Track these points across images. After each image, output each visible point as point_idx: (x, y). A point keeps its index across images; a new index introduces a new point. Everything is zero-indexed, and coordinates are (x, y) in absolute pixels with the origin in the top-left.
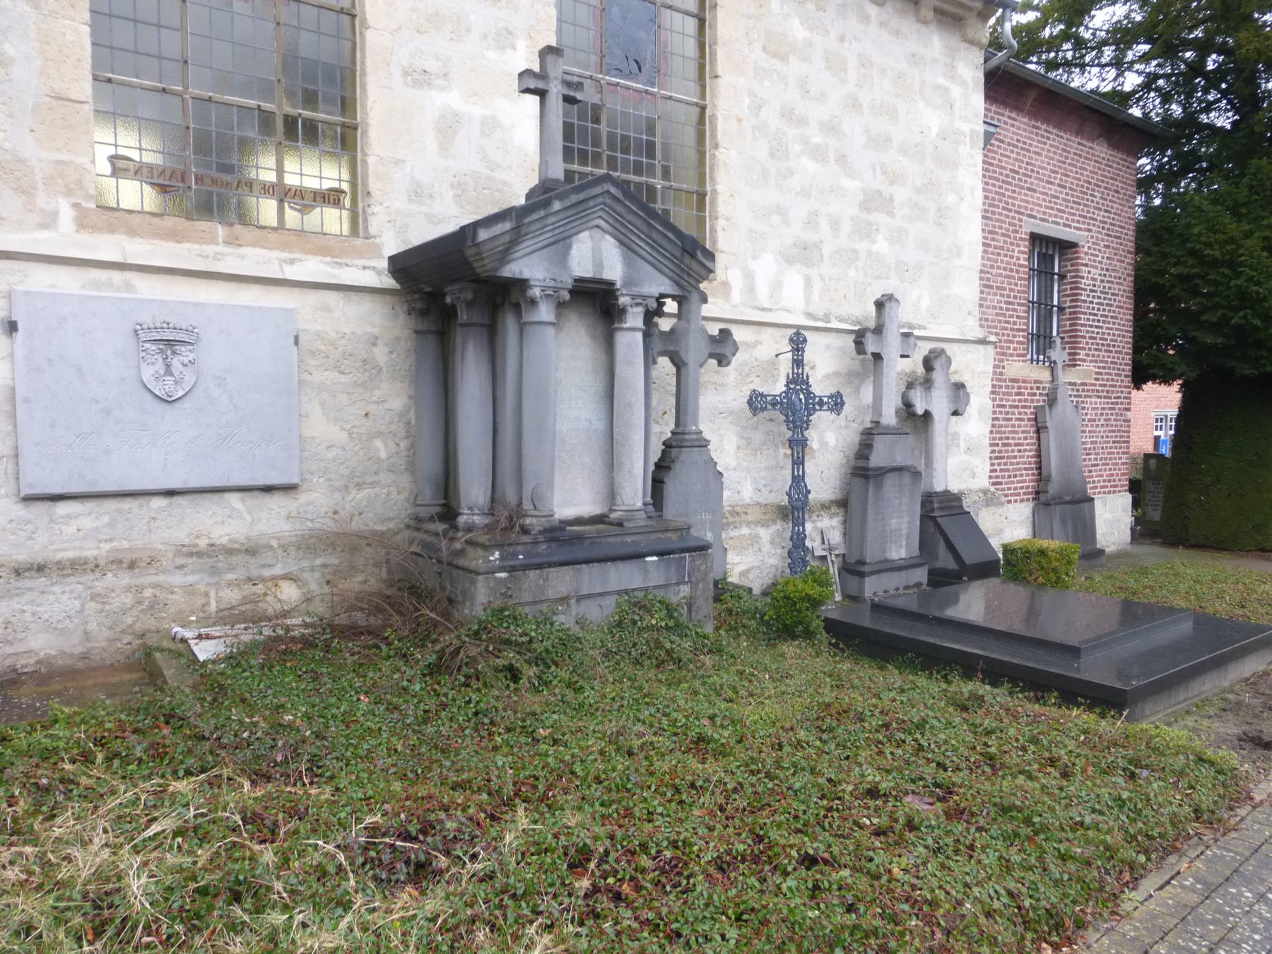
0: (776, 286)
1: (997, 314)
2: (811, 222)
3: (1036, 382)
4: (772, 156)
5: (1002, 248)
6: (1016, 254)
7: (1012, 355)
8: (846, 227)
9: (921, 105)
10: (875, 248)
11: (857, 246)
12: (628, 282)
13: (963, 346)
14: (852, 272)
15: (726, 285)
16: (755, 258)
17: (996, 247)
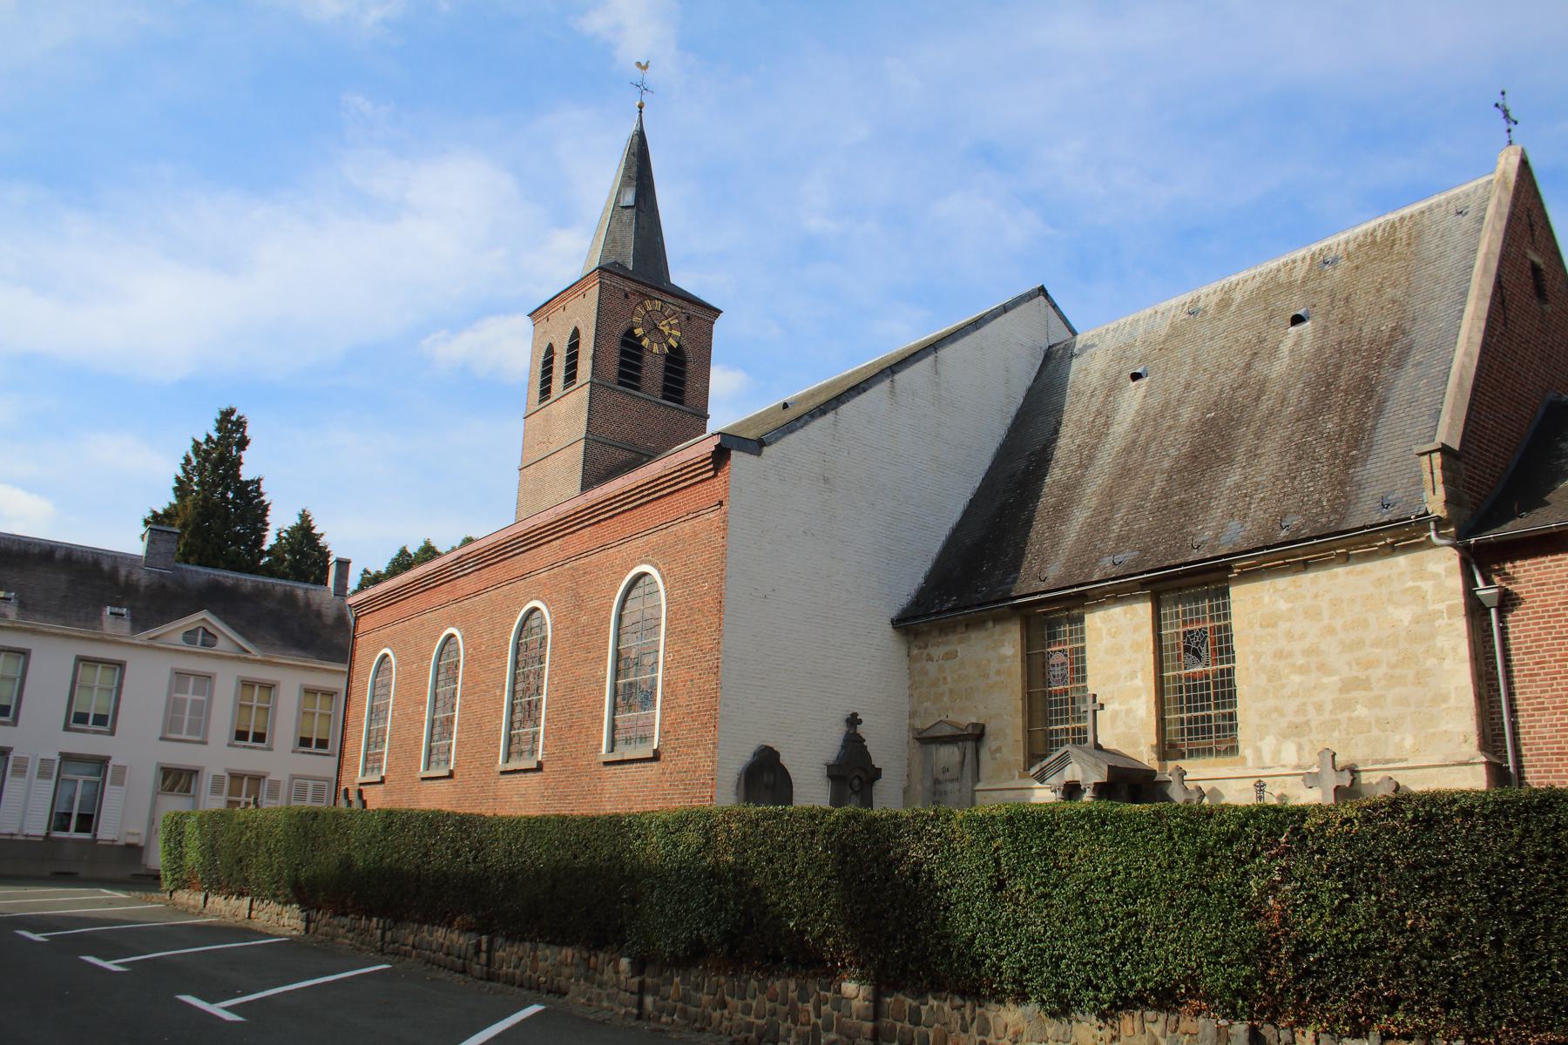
1: (1557, 731)
2: (1301, 710)
4: (1269, 680)
8: (1329, 707)
9: (1391, 609)
10: (1355, 714)
11: (1339, 717)
12: (1083, 780)
13: (1446, 770)
14: (1336, 734)
15: (1244, 758)
16: (1262, 739)
17: (1546, 674)
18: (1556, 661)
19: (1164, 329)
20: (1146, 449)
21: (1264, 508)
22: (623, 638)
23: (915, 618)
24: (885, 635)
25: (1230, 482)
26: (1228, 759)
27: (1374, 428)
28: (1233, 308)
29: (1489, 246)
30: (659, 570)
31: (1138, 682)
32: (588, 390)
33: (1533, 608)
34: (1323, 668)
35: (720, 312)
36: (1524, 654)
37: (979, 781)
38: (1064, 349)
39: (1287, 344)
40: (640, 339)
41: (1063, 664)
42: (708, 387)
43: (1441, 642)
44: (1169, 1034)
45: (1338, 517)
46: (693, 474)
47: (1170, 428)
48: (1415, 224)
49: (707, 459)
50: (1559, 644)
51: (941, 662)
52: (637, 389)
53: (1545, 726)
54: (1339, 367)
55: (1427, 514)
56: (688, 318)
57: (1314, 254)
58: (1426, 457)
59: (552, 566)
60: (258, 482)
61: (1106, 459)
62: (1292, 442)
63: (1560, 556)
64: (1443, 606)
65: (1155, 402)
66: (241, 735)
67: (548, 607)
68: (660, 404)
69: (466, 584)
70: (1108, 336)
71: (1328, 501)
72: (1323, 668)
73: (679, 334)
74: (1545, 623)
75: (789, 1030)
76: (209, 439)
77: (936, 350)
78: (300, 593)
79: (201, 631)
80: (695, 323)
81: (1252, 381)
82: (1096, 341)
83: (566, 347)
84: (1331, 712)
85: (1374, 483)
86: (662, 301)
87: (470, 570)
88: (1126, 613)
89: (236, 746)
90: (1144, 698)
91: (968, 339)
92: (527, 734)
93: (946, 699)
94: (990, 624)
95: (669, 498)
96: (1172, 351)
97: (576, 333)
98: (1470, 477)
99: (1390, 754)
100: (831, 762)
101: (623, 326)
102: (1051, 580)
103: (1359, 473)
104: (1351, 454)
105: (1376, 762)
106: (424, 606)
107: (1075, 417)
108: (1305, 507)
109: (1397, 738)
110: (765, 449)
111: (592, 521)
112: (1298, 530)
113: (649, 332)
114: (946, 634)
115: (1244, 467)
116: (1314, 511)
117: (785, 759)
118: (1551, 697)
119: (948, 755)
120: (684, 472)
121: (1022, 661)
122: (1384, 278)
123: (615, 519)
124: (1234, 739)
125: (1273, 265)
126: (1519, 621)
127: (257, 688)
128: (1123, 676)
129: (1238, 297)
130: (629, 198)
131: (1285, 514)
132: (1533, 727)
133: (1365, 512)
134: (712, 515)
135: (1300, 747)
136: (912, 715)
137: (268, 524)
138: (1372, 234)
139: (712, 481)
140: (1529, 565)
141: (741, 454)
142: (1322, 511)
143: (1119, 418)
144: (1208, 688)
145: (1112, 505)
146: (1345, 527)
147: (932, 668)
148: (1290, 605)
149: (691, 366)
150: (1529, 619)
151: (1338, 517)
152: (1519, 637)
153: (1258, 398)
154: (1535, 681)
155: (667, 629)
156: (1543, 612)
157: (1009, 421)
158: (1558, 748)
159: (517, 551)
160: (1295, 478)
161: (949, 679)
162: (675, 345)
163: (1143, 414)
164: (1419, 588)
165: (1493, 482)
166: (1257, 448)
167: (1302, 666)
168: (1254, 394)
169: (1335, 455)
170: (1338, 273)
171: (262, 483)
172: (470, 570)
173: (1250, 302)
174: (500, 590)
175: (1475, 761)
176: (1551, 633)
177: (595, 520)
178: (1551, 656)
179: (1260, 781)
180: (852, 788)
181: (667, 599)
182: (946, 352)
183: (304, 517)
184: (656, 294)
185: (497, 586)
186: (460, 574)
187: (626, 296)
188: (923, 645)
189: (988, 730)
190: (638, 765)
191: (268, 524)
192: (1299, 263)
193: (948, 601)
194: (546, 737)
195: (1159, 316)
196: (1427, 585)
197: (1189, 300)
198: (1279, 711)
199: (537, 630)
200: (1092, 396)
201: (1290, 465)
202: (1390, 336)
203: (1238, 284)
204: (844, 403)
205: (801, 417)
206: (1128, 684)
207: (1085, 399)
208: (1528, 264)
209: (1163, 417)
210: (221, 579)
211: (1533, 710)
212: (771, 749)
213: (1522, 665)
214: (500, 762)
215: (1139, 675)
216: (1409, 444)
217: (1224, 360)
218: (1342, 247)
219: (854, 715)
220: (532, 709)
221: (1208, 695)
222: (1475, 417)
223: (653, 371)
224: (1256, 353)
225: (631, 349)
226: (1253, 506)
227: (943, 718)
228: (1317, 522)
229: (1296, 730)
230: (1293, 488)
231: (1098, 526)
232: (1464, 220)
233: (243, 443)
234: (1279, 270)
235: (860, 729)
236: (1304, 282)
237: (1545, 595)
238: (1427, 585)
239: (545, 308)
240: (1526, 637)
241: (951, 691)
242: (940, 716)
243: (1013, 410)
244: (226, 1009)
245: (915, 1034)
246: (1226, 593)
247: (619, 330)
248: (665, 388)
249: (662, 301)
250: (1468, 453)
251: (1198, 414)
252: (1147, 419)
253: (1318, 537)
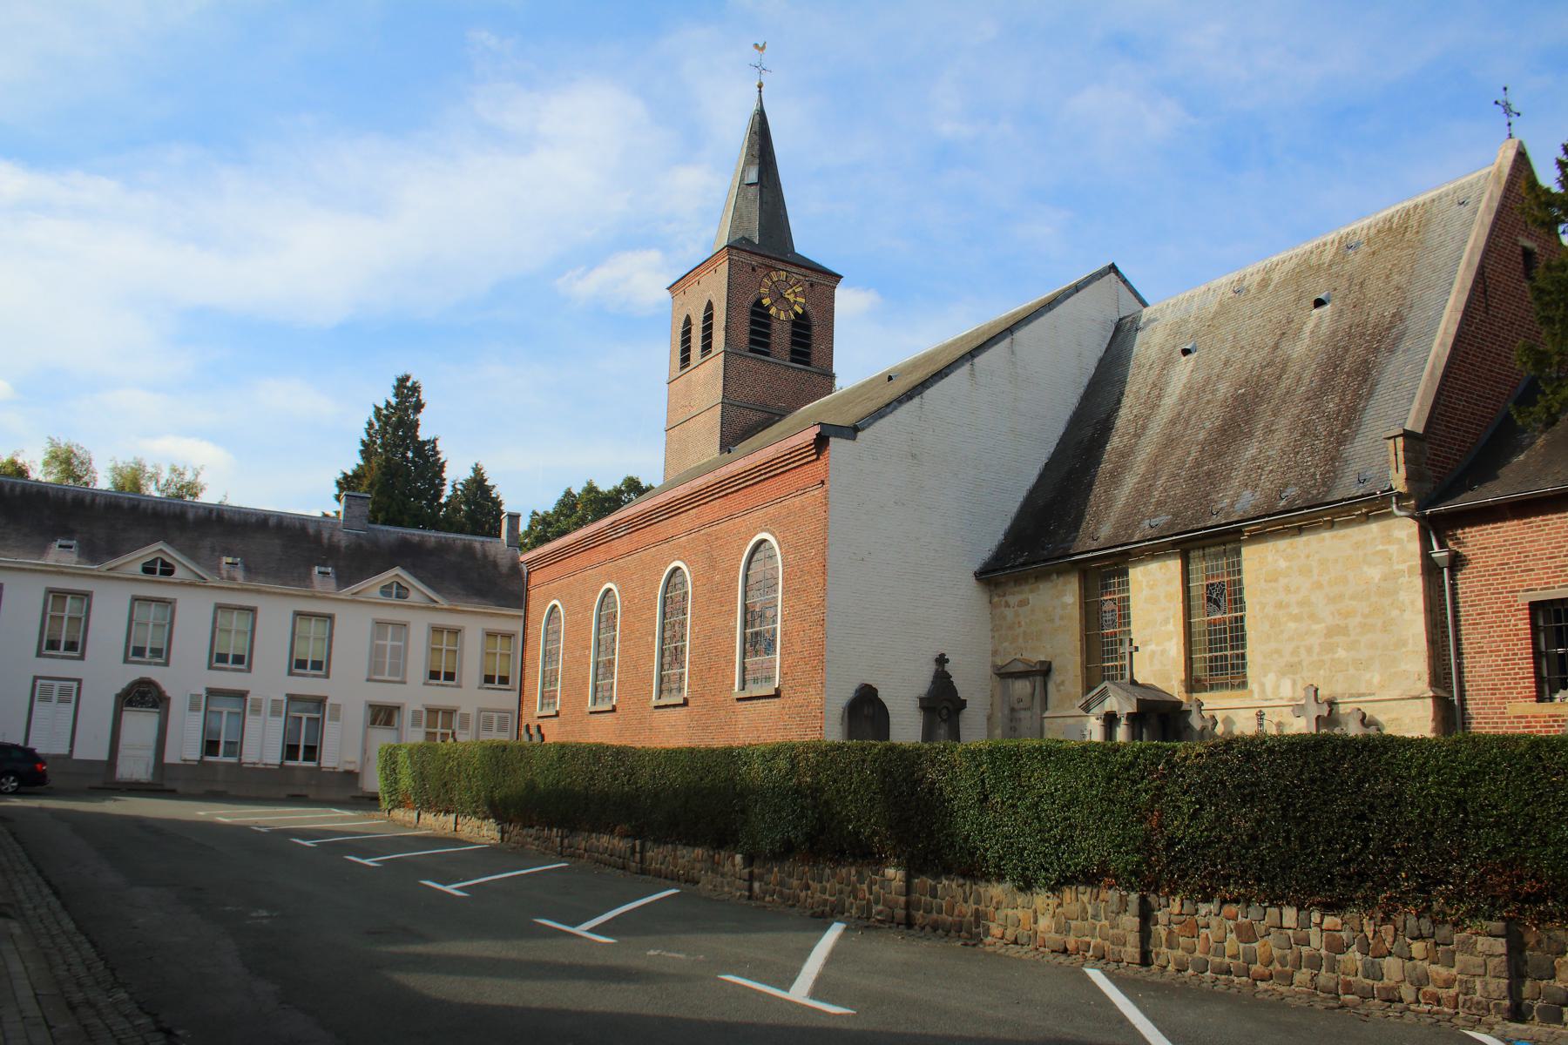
0: (1277, 687)
1: (1492, 670)
2: (1295, 652)
3: (1550, 716)
5: (1496, 622)
6: (1513, 622)
7: (1517, 698)
8: (1316, 649)
9: (1365, 569)
10: (1337, 656)
12: (1119, 710)
13: (1403, 702)
14: (1322, 672)
15: (1251, 691)
16: (1265, 676)
18: (1493, 613)
19: (1214, 307)
20: (1187, 421)
21: (1271, 479)
22: (750, 594)
23: (994, 571)
24: (969, 587)
25: (1248, 455)
26: (1240, 692)
27: (1364, 408)
28: (1271, 288)
29: (1476, 240)
30: (776, 537)
31: (1170, 627)
32: (723, 358)
33: (1477, 567)
34: (1313, 617)
35: (841, 277)
36: (1469, 606)
37: (1047, 709)
38: (1132, 321)
39: (1310, 325)
40: (768, 308)
41: (1113, 611)
42: (832, 348)
43: (1403, 596)
44: (1093, 901)
45: (1325, 489)
46: (800, 457)
47: (1208, 402)
48: (1426, 212)
49: (811, 444)
50: (1495, 598)
51: (1016, 608)
52: (767, 354)
53: (1484, 667)
54: (1346, 350)
55: (1391, 489)
56: (812, 285)
57: (1342, 237)
58: (1392, 441)
59: (690, 532)
60: (434, 441)
61: (1155, 430)
62: (1300, 419)
63: (1499, 525)
64: (1404, 567)
65: (1199, 377)
66: (434, 675)
67: (688, 567)
68: (789, 367)
69: (620, 546)
70: (1169, 311)
71: (1321, 474)
72: (1313, 617)
73: (803, 301)
74: (1486, 580)
75: (852, 904)
76: (388, 404)
77: (1012, 333)
78: (477, 545)
79: (395, 585)
80: (818, 289)
81: (1278, 360)
82: (1158, 315)
83: (702, 319)
84: (1318, 654)
85: (1356, 460)
86: (787, 271)
87: (622, 533)
88: (1161, 569)
89: (431, 685)
90: (1174, 641)
91: (1042, 320)
92: (674, 674)
93: (1021, 640)
94: (1055, 576)
95: (782, 476)
96: (1218, 328)
97: (710, 306)
98: (1435, 455)
99: (1363, 690)
100: (923, 696)
101: (752, 298)
102: (1102, 540)
103: (1349, 450)
104: (1344, 432)
105: (1351, 696)
106: (586, 564)
107: (1134, 389)
108: (1302, 480)
109: (1368, 676)
110: (859, 433)
111: (721, 494)
112: (1295, 500)
113: (776, 301)
114: (1020, 585)
115: (1260, 442)
116: (1309, 483)
117: (882, 695)
118: (1489, 642)
119: (1022, 687)
120: (792, 455)
121: (1080, 608)
122: (1394, 265)
123: (739, 493)
124: (1245, 676)
125: (1308, 247)
126: (1465, 578)
127: (445, 633)
128: (1159, 622)
129: (1276, 277)
130: (753, 176)
131: (1286, 486)
132: (1475, 667)
133: (1348, 487)
134: (816, 492)
135: (1294, 683)
136: (995, 653)
137: (445, 480)
138: (1390, 220)
139: (815, 463)
140: (1475, 532)
141: (836, 439)
142: (1315, 483)
143: (1169, 390)
144: (1225, 633)
145: (1156, 472)
146: (1329, 499)
147: (1009, 613)
148: (1288, 564)
149: (816, 330)
150: (1474, 577)
151: (1325, 489)
152: (1466, 592)
153: (1279, 378)
154: (1477, 629)
155: (783, 588)
156: (1485, 571)
157: (1082, 390)
158: (1493, 685)
159: (661, 518)
160: (1298, 453)
161: (1023, 623)
162: (800, 311)
163: (1189, 387)
164: (1387, 551)
165: (1460, 456)
166: (1272, 425)
167: (1296, 614)
168: (1278, 372)
169: (1331, 434)
170: (1358, 257)
171: (438, 443)
172: (622, 533)
173: (1284, 283)
174: (648, 551)
175: (1425, 695)
176: (1490, 589)
177: (724, 493)
178: (1490, 608)
179: (1260, 711)
180: (941, 718)
181: (783, 563)
182: (1022, 334)
183: (477, 470)
184: (780, 265)
185: (646, 547)
186: (615, 536)
187: (753, 269)
188: (1002, 594)
189: (1054, 665)
190: (764, 701)
191: (445, 480)
192: (1328, 246)
193: (1021, 556)
194: (689, 677)
195: (1211, 293)
196: (1393, 549)
197: (1237, 278)
198: (1278, 652)
199: (680, 586)
200: (1150, 369)
201: (1296, 441)
202: (1391, 322)
203: (1277, 265)
204: (928, 388)
205: (891, 402)
206: (1163, 628)
207: (1144, 371)
208: (1519, 251)
209: (1204, 391)
210: (408, 536)
211: (1475, 653)
212: (870, 686)
213: (1468, 615)
214: (654, 699)
215: (1171, 621)
216: (1389, 425)
217: (1258, 339)
218: (1365, 232)
219: (942, 655)
220: (678, 652)
221: (1226, 638)
222: (1445, 400)
223: (781, 337)
224: (1284, 334)
225: (760, 318)
226: (1263, 477)
227: (1018, 656)
228: (1309, 493)
229: (1292, 668)
230: (1296, 462)
231: (1142, 493)
232: (1465, 210)
233: (419, 407)
234: (1312, 253)
235: (948, 667)
236: (1330, 266)
237: (1486, 557)
238: (1393, 549)
239: (681, 282)
240: (1471, 592)
241: (1025, 632)
242: (1016, 654)
243: (1085, 381)
244: (456, 889)
245: (934, 904)
246: (1239, 553)
247: (748, 303)
248: (793, 352)
249: (787, 271)
250: (1433, 433)
251: (1232, 389)
252: (1194, 392)
253: (1308, 508)
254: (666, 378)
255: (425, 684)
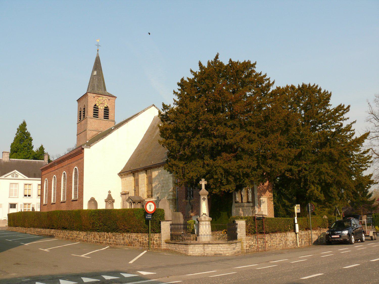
40: (98, 106)
43: (170, 181)
52: (98, 117)
69: (56, 167)
80: (110, 100)
101: (94, 104)
106: (51, 171)
149: (110, 111)
162: (106, 106)
184: (101, 96)
187: (94, 97)
219: (110, 191)
223: (101, 113)
239: (83, 97)
254: (77, 122)
255: (23, 198)
